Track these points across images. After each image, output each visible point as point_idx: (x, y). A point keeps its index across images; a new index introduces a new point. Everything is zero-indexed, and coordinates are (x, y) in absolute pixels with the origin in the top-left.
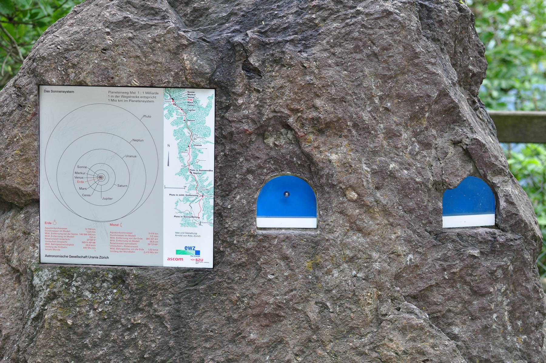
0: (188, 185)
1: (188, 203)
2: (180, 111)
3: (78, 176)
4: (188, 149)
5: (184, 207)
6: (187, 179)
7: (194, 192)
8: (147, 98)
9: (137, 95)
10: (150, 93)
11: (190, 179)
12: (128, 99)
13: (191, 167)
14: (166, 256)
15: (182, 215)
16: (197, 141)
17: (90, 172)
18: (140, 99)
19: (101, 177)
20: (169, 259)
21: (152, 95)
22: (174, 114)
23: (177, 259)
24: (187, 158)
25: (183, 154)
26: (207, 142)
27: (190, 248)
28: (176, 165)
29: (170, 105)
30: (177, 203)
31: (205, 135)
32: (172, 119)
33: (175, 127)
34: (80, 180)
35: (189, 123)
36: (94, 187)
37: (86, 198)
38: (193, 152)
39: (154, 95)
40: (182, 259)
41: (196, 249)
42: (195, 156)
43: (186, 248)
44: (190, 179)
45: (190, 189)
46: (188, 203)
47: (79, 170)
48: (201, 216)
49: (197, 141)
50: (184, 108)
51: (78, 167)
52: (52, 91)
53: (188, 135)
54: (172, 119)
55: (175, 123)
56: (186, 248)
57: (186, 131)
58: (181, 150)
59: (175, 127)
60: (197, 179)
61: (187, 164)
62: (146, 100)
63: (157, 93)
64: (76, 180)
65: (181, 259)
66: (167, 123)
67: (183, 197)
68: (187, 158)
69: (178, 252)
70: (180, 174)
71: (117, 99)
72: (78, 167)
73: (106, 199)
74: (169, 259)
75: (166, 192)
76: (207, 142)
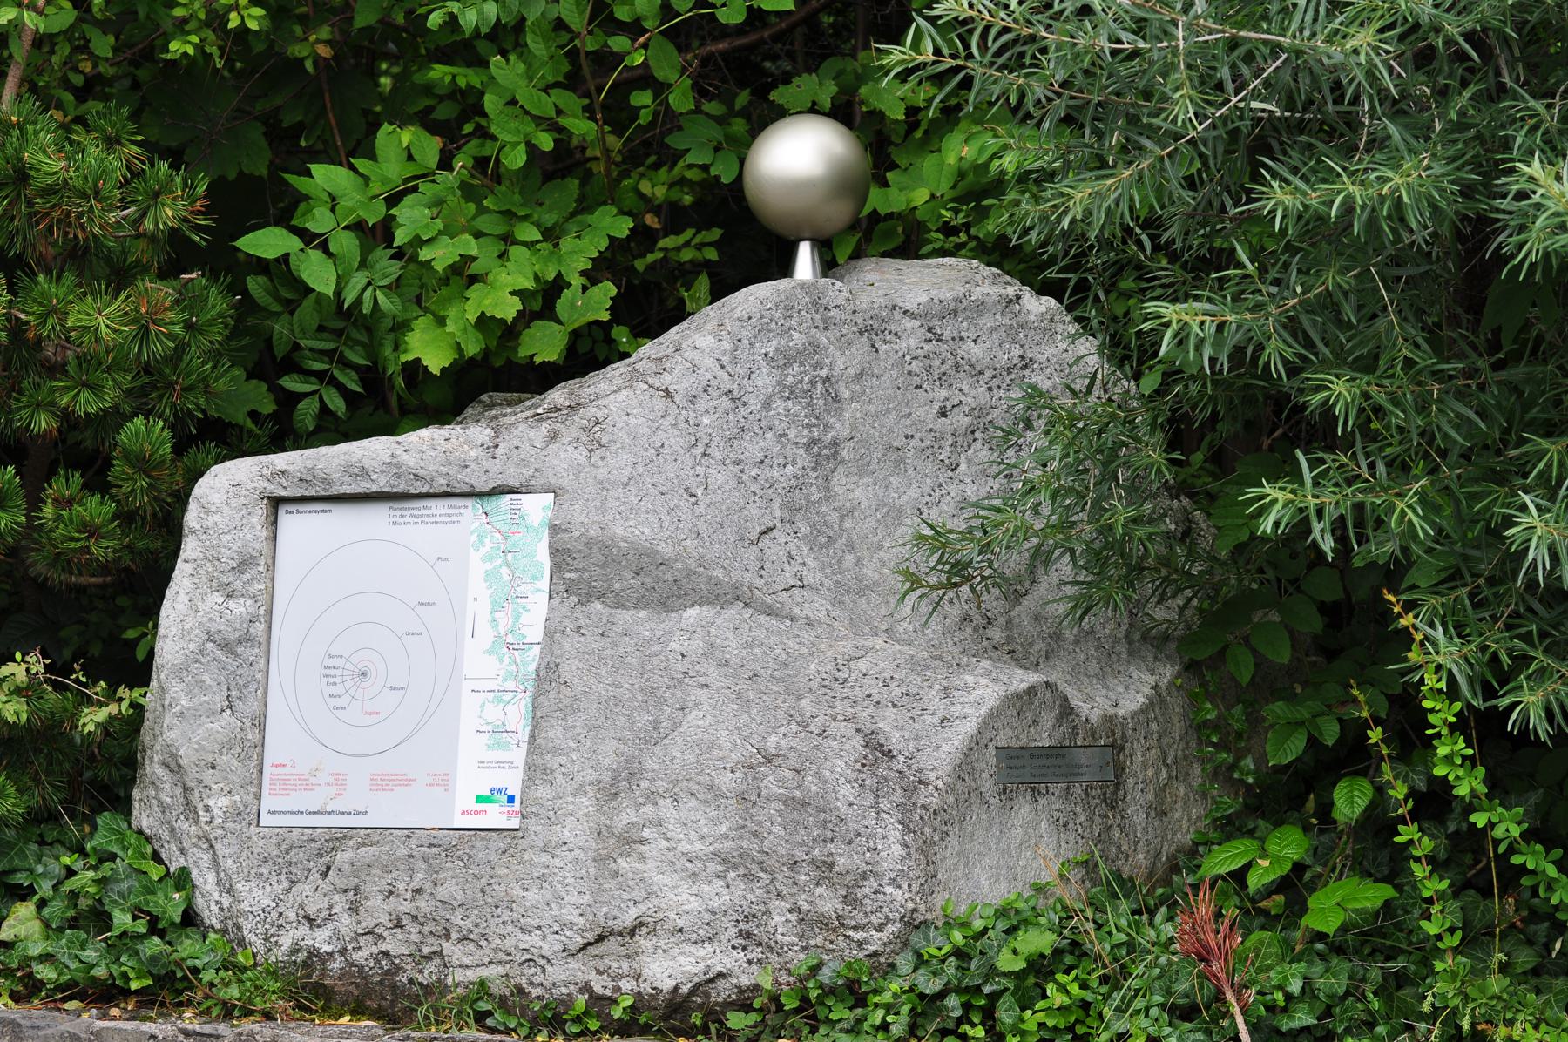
0: (502, 673)
1: (502, 705)
2: (497, 535)
3: (328, 673)
4: (505, 604)
5: (494, 714)
6: (501, 661)
7: (510, 685)
8: (450, 516)
9: (434, 511)
10: (455, 507)
11: (507, 660)
12: (419, 520)
13: (510, 639)
14: (459, 807)
15: (490, 728)
16: (522, 590)
17: (348, 666)
18: (438, 519)
19: (364, 674)
20: (464, 813)
21: (457, 511)
22: (487, 541)
23: (477, 813)
24: (504, 620)
25: (497, 615)
26: (538, 590)
27: (499, 791)
28: (486, 635)
29: (482, 524)
30: (482, 706)
31: (535, 578)
32: (483, 551)
33: (488, 566)
34: (331, 680)
35: (510, 556)
36: (352, 692)
37: (339, 713)
38: (514, 611)
39: (462, 511)
40: (484, 812)
41: (509, 792)
42: (517, 618)
43: (492, 790)
44: (507, 660)
45: (505, 680)
46: (502, 705)
47: (330, 662)
48: (520, 730)
49: (522, 590)
50: (504, 528)
51: (330, 656)
52: (298, 512)
53: (508, 578)
54: (483, 551)
55: (488, 558)
56: (492, 790)
57: (505, 571)
58: (496, 608)
59: (488, 566)
60: (518, 660)
61: (503, 633)
62: (447, 519)
63: (466, 507)
64: (325, 680)
65: (484, 812)
66: (475, 557)
67: (492, 694)
68: (504, 620)
69: (480, 799)
70: (488, 652)
71: (402, 520)
72: (330, 656)
73: (370, 714)
74: (464, 813)
75: (467, 686)
76: (538, 590)
